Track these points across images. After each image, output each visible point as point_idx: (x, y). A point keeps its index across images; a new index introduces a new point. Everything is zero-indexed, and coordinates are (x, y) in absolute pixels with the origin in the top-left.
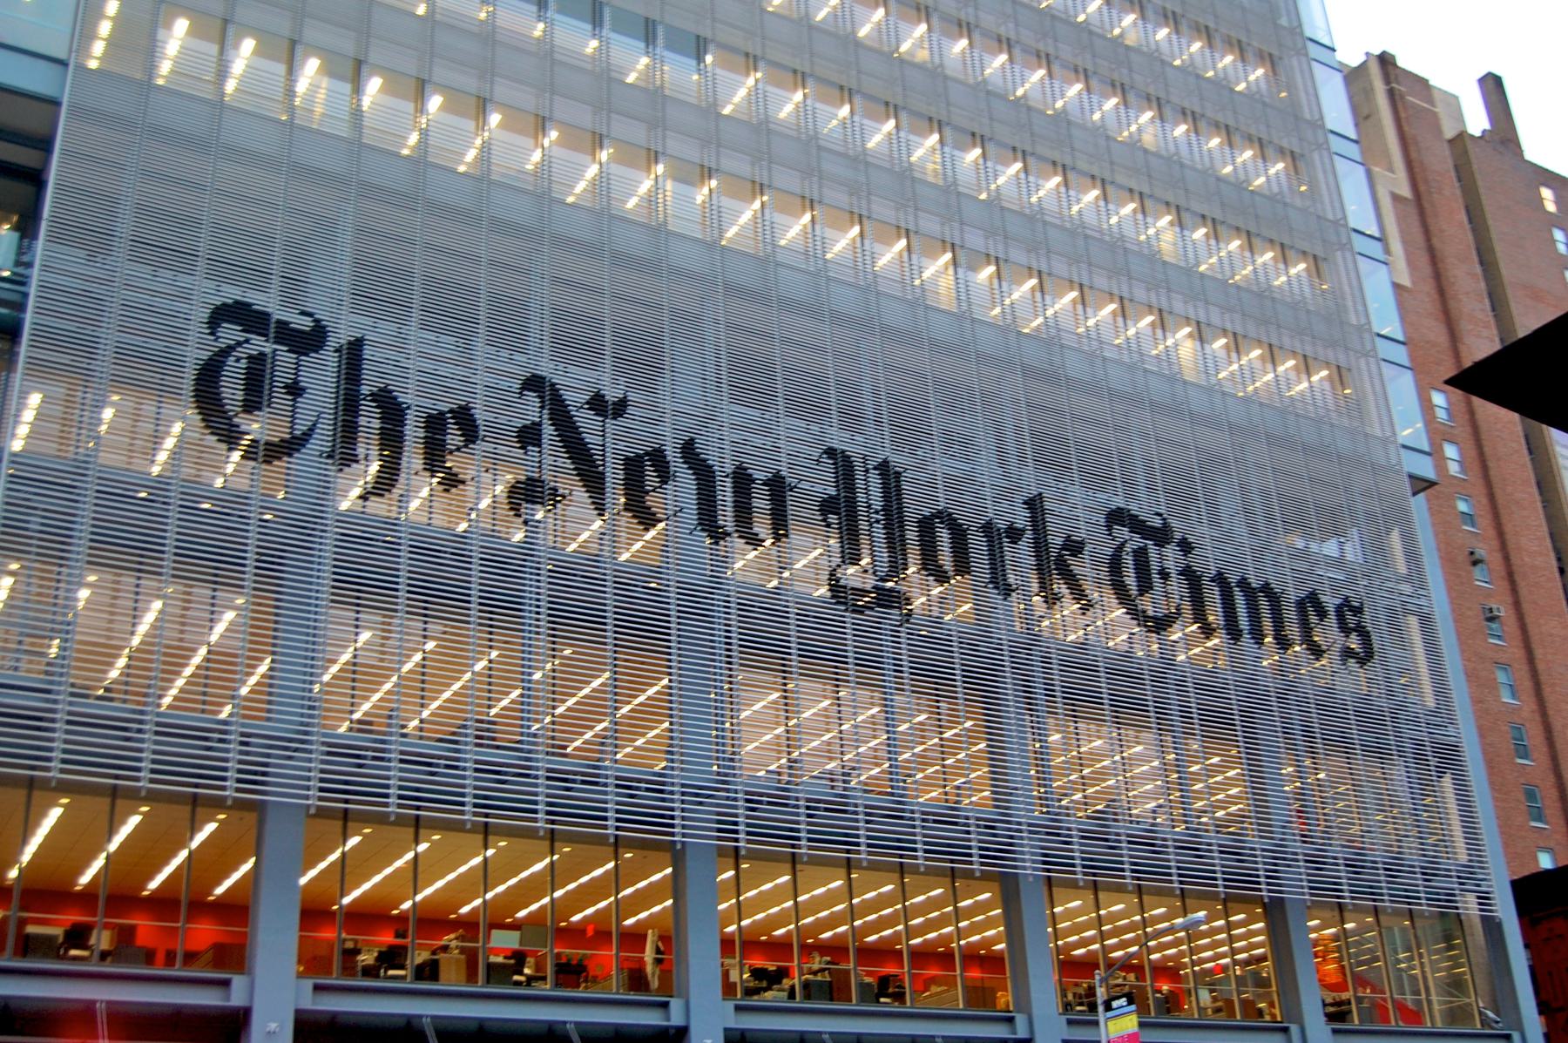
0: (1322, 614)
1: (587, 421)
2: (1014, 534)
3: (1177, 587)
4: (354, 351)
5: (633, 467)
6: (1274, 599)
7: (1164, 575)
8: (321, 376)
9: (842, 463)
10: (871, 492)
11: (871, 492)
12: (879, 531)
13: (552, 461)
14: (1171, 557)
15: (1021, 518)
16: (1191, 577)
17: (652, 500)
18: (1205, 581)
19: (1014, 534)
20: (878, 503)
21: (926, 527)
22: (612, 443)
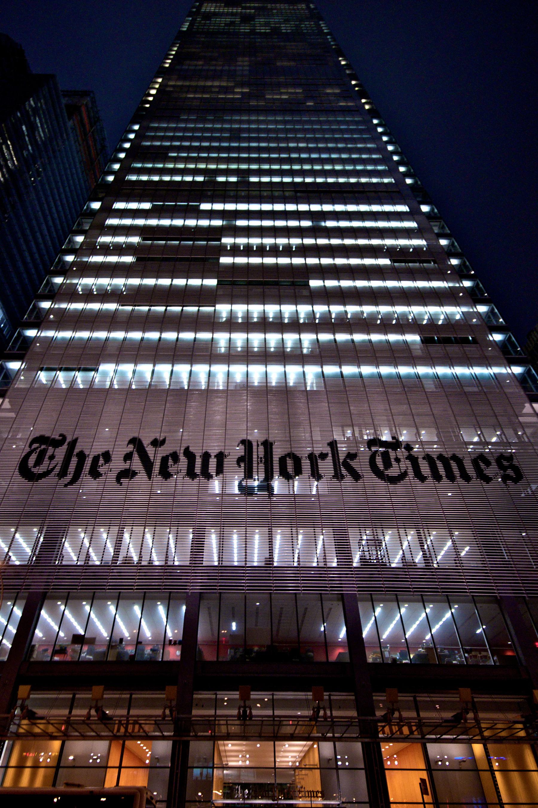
0: (488, 463)
1: (150, 450)
2: (323, 456)
3: (406, 465)
4: (74, 443)
5: (164, 460)
6: (459, 462)
7: (398, 460)
8: (61, 452)
9: (247, 444)
10: (258, 452)
11: (258, 452)
12: (262, 466)
13: (137, 464)
14: (401, 453)
15: (328, 450)
16: (413, 460)
17: (171, 470)
18: (420, 461)
19: (323, 456)
20: (262, 454)
21: (283, 460)
22: (156, 455)
